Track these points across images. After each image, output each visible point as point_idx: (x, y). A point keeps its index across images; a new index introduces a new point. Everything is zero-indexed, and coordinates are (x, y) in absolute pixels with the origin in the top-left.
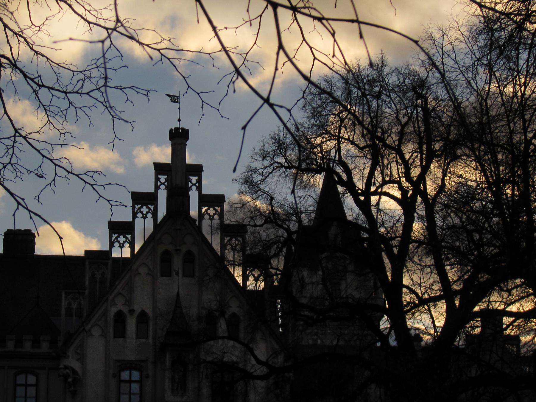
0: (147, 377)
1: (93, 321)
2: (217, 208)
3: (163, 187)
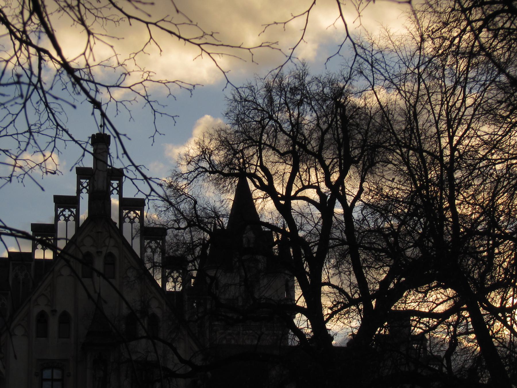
2: (137, 212)
3: (85, 191)
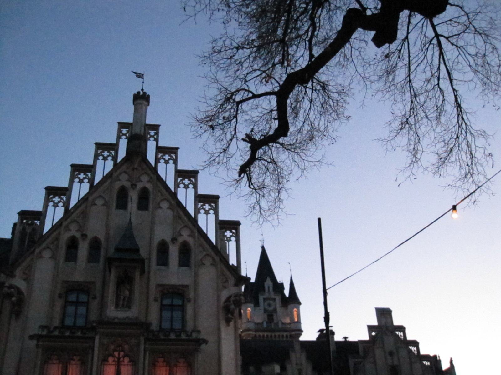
0: (95, 298)
1: (44, 245)
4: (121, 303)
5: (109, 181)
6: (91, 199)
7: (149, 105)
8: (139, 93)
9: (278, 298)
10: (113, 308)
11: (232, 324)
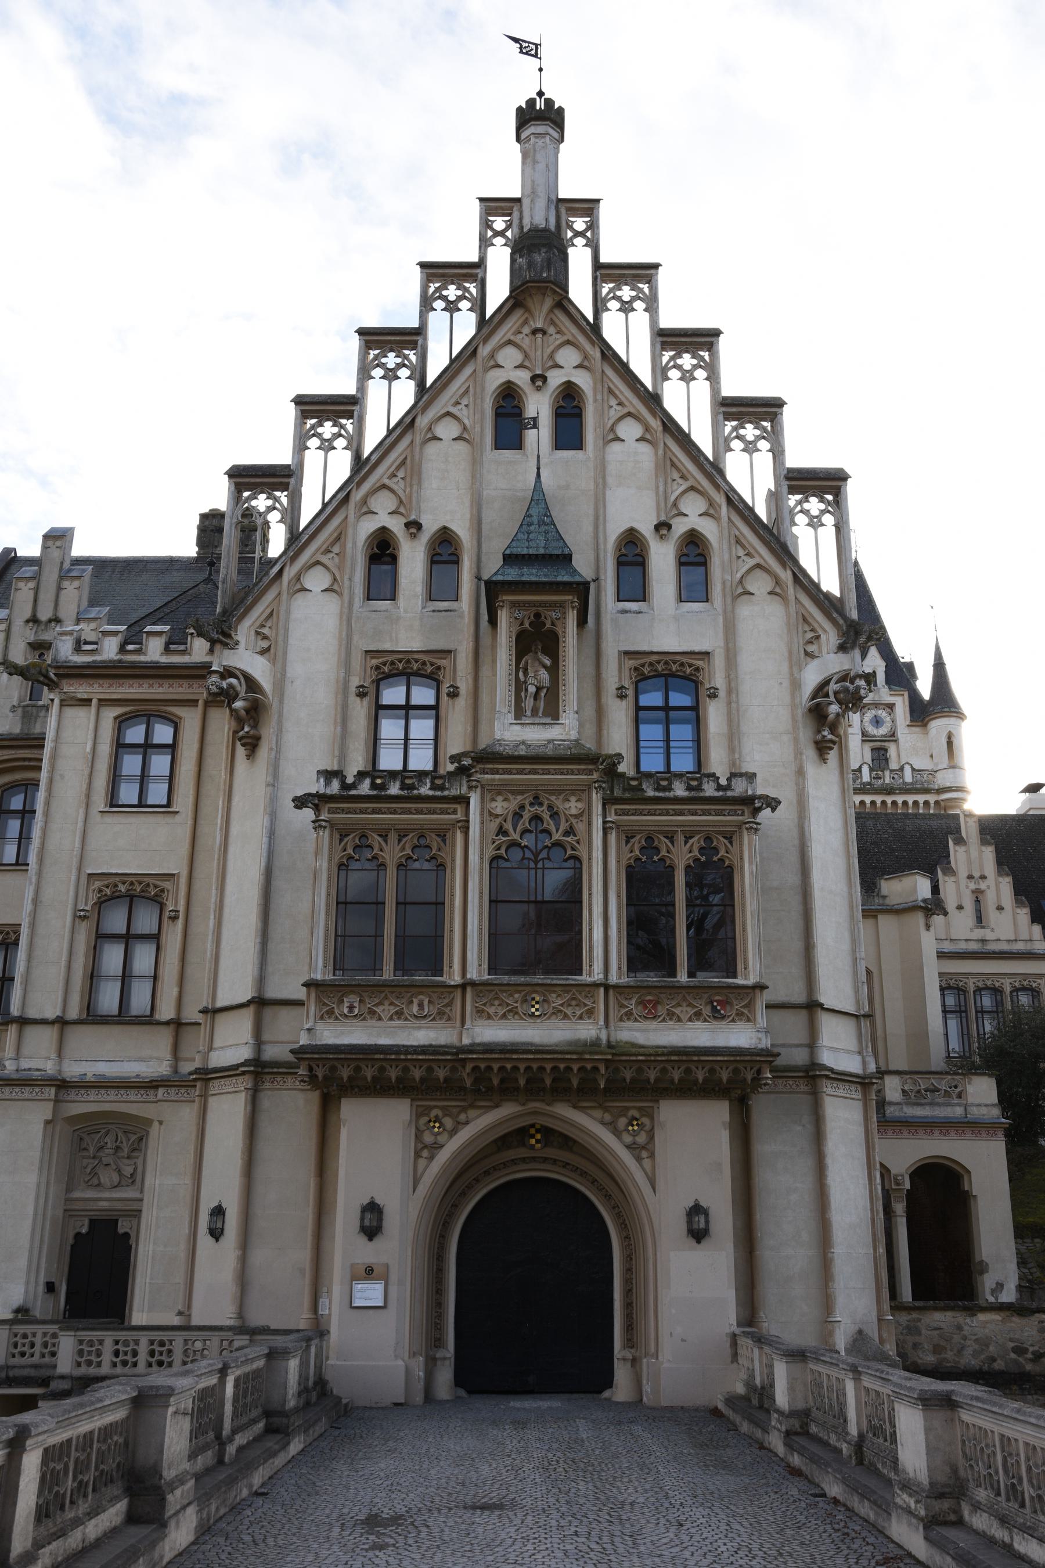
0: (454, 694)
4: (529, 703)
5: (467, 371)
6: (422, 422)
7: (562, 140)
8: (531, 102)
9: (901, 705)
10: (510, 718)
11: (833, 755)
